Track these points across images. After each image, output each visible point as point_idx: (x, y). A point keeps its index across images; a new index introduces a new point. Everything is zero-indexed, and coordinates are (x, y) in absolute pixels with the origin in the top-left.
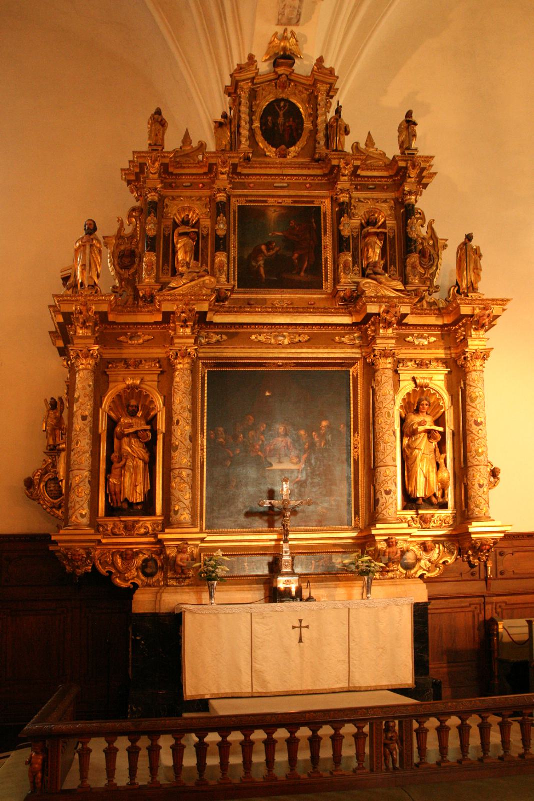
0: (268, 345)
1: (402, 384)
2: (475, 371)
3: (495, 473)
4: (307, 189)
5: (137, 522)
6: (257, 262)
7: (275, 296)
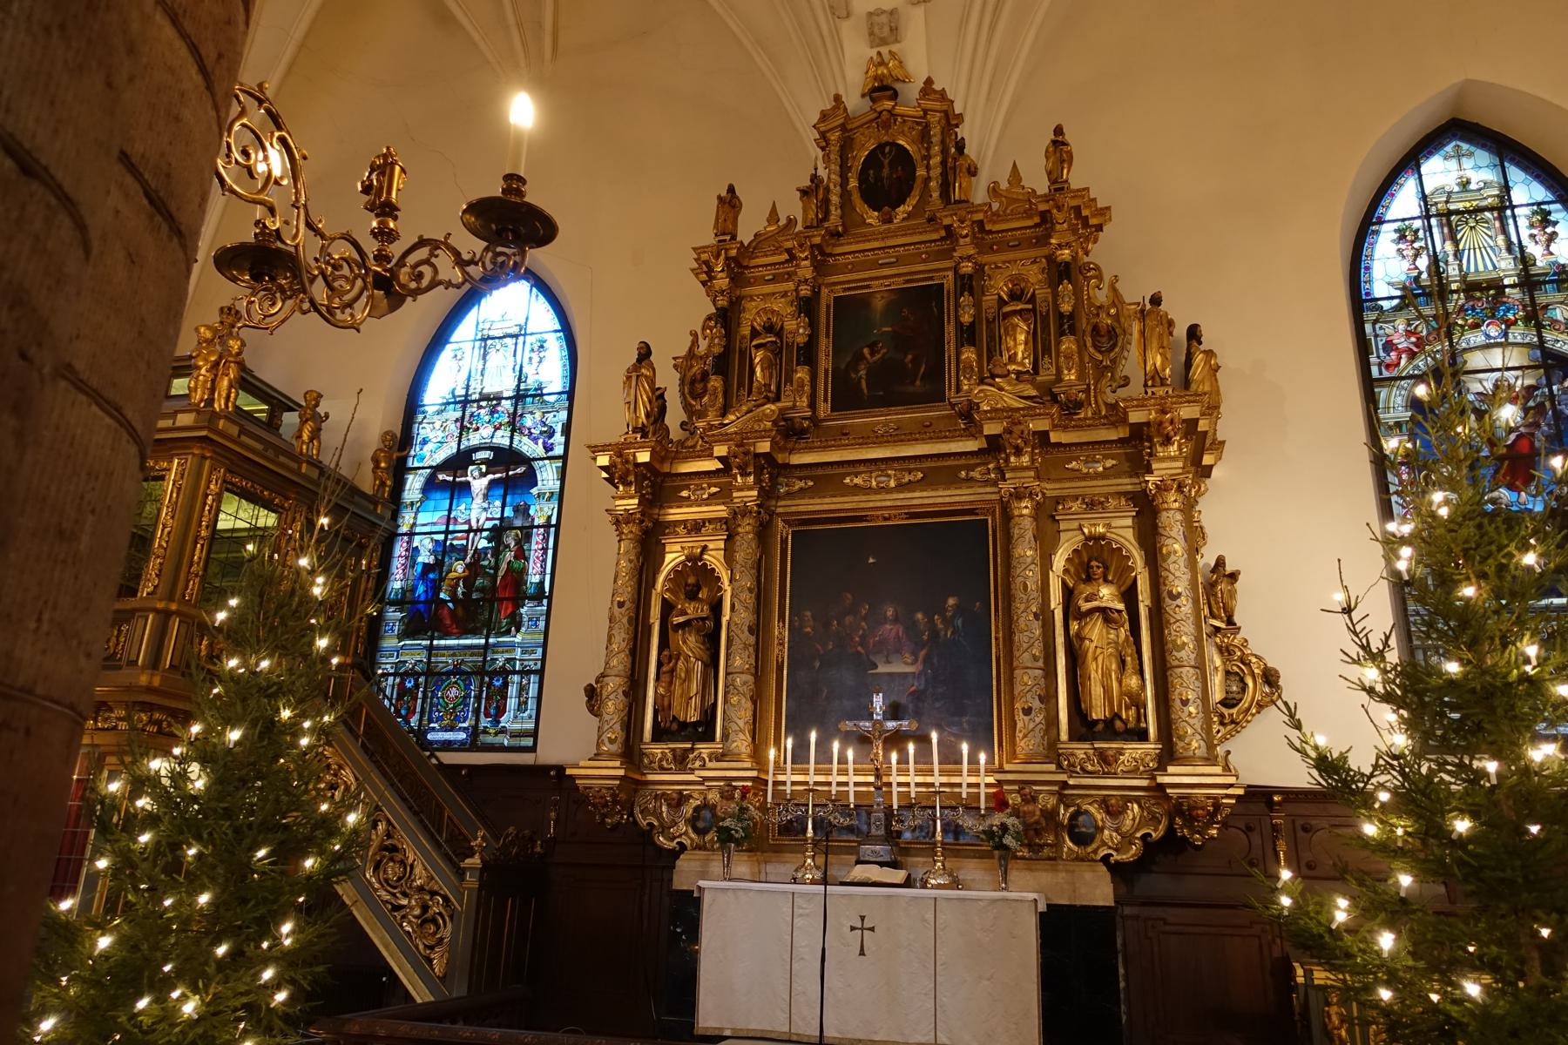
0: (868, 490)
2: (1166, 510)
4: (925, 261)
6: (857, 372)
7: (880, 419)
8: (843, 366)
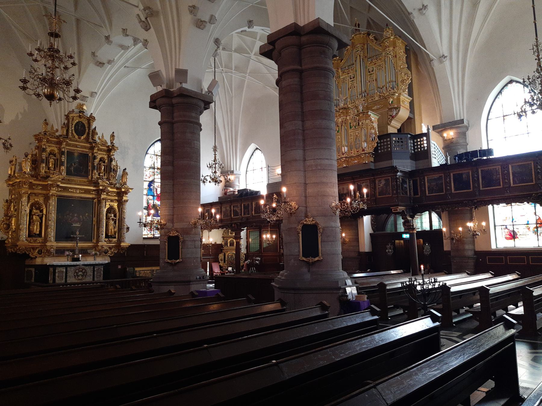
1: (107, 206)
3: (128, 228)
5: (37, 239)
8: (68, 166)
